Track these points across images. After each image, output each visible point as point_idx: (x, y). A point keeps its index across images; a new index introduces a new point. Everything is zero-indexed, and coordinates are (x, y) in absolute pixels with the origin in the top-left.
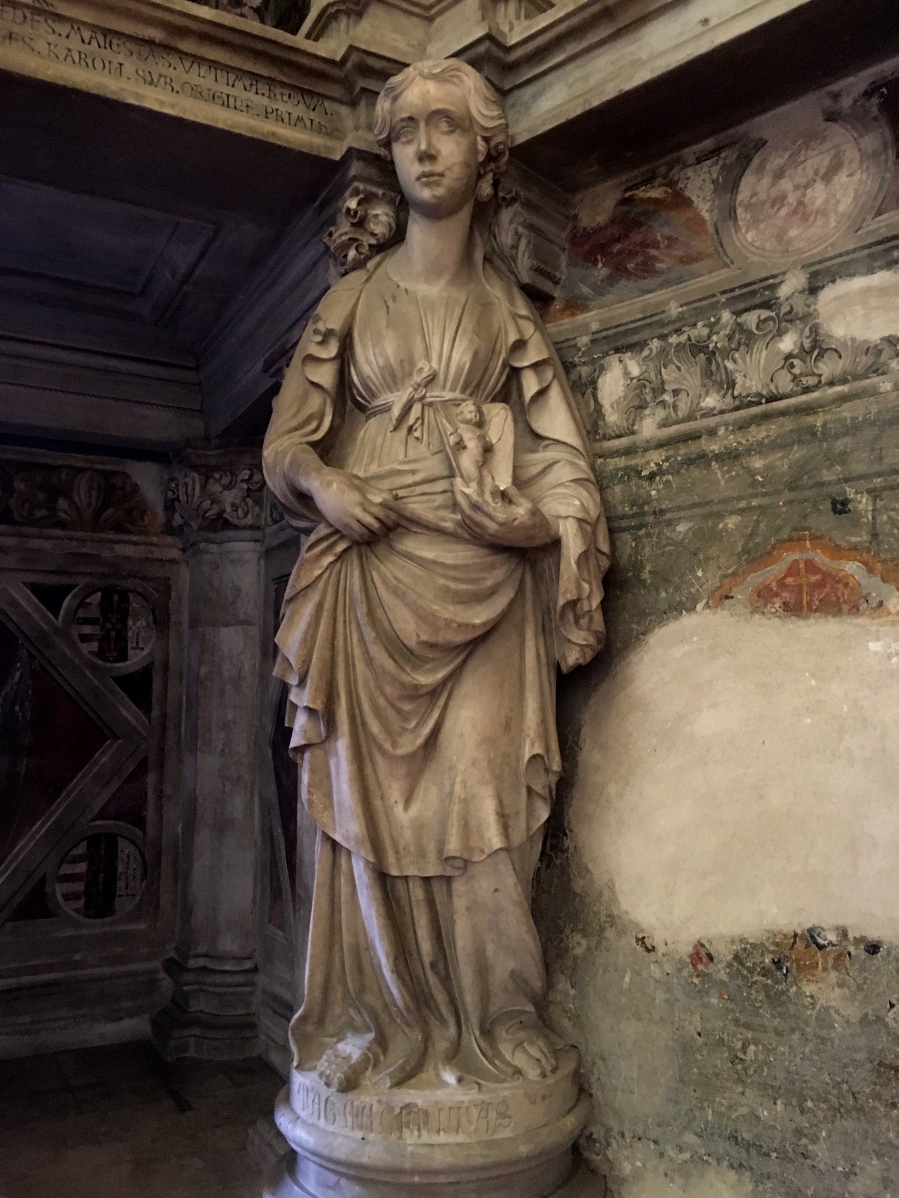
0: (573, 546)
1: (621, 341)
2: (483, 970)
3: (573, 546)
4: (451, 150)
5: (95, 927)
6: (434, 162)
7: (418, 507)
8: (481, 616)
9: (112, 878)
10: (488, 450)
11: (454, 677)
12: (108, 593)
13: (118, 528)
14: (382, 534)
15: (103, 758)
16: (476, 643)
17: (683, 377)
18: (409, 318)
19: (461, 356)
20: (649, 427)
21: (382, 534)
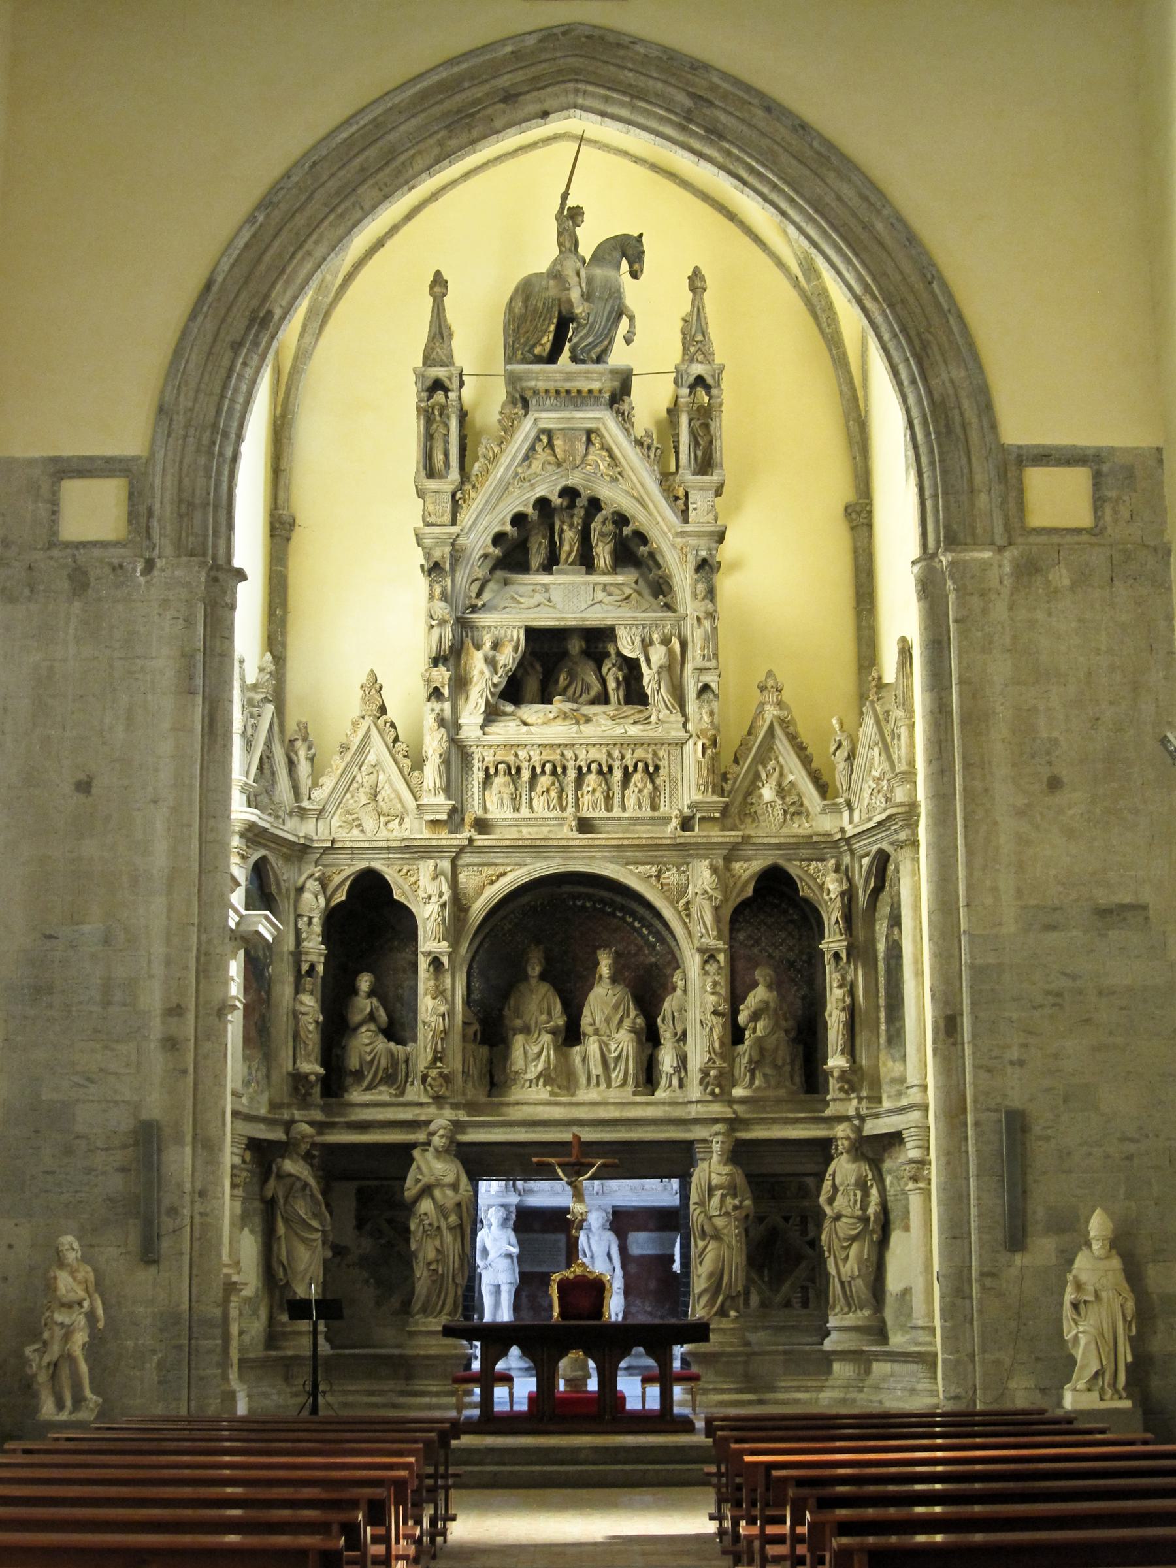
0: (872, 1219)
1: (889, 1172)
2: (859, 1297)
3: (872, 1219)
4: (846, 1143)
5: (804, 1311)
6: (842, 1145)
7: (844, 1212)
8: (854, 1232)
9: (808, 1299)
10: (856, 1201)
11: (850, 1246)
12: (802, 1217)
13: (803, 1197)
14: (838, 1217)
15: (803, 1264)
16: (853, 1239)
17: (895, 1181)
18: (844, 1169)
19: (853, 1180)
20: (892, 1193)
21: (838, 1217)
